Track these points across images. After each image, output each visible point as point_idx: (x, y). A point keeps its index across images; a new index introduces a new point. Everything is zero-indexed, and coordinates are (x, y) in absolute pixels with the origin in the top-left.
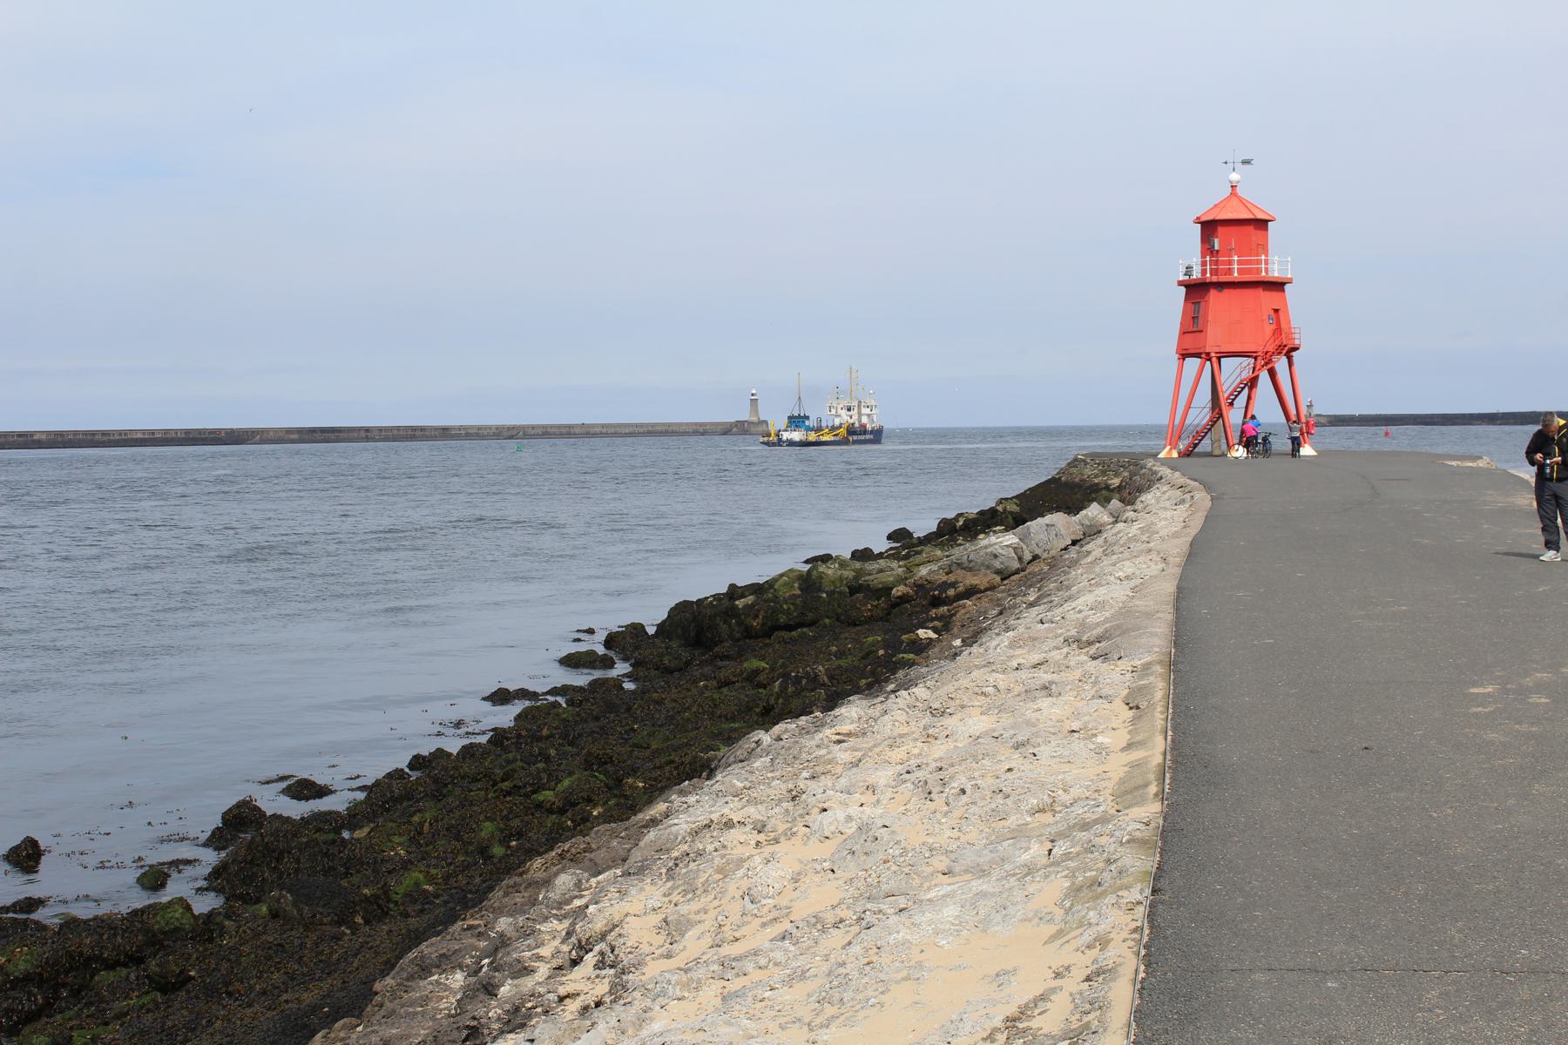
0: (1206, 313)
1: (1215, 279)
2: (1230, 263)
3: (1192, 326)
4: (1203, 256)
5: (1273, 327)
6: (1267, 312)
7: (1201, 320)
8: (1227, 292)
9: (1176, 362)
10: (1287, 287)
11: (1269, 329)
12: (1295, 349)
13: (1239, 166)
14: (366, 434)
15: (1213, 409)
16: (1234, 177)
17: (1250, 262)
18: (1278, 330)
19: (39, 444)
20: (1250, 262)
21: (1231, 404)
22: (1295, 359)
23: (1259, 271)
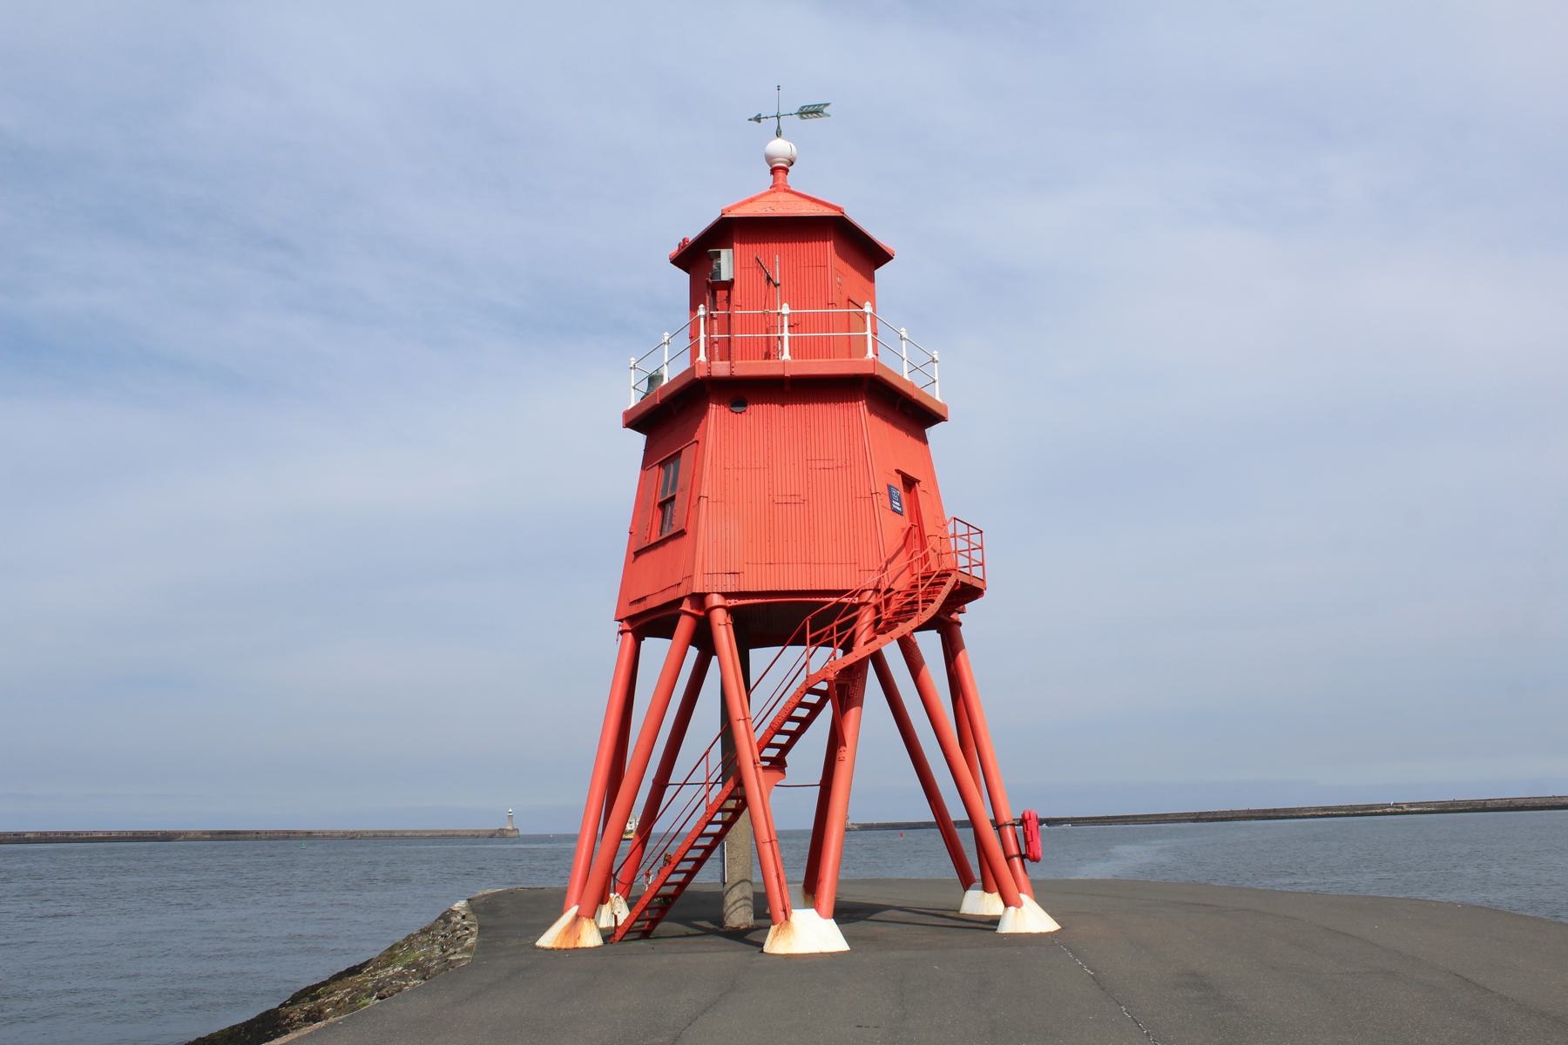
0: (696, 478)
1: (721, 369)
2: (770, 323)
3: (662, 524)
4: (694, 308)
5: (904, 522)
6: (884, 478)
7: (680, 504)
8: (758, 414)
9: (609, 641)
10: (932, 432)
11: (893, 527)
12: (968, 592)
13: (791, 123)
14: (91, 838)
15: (725, 776)
16: (780, 147)
17: (827, 323)
18: (915, 535)
19: (29, 841)
20: (827, 323)
21: (778, 764)
22: (964, 631)
23: (854, 347)
